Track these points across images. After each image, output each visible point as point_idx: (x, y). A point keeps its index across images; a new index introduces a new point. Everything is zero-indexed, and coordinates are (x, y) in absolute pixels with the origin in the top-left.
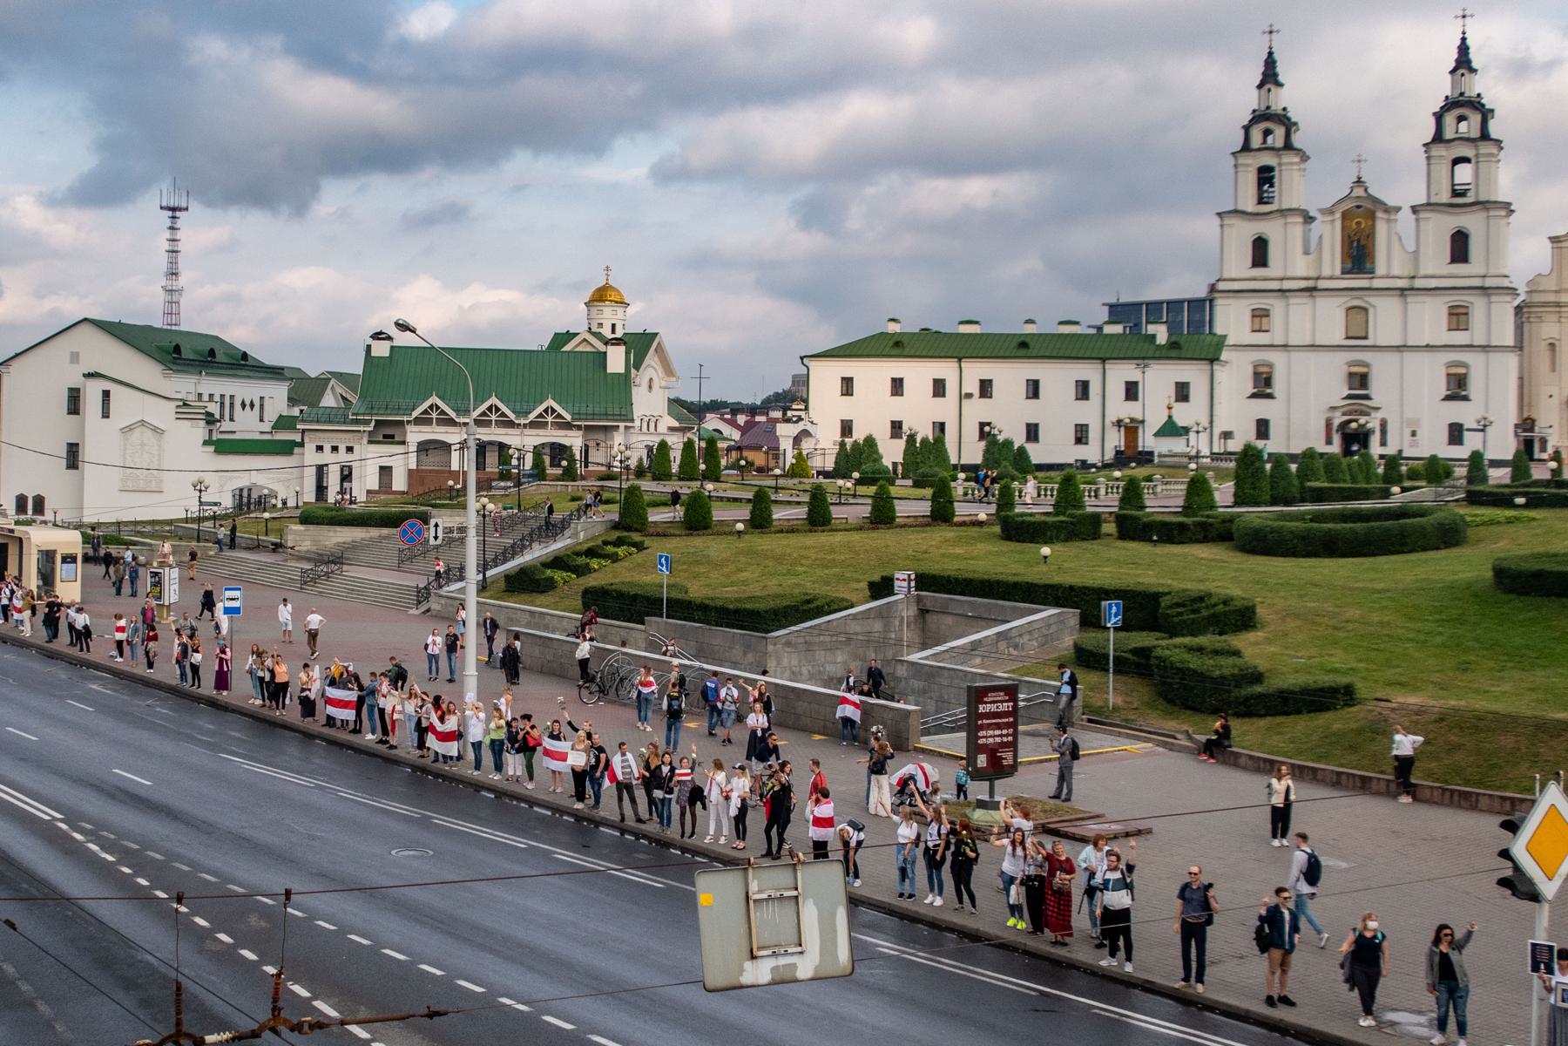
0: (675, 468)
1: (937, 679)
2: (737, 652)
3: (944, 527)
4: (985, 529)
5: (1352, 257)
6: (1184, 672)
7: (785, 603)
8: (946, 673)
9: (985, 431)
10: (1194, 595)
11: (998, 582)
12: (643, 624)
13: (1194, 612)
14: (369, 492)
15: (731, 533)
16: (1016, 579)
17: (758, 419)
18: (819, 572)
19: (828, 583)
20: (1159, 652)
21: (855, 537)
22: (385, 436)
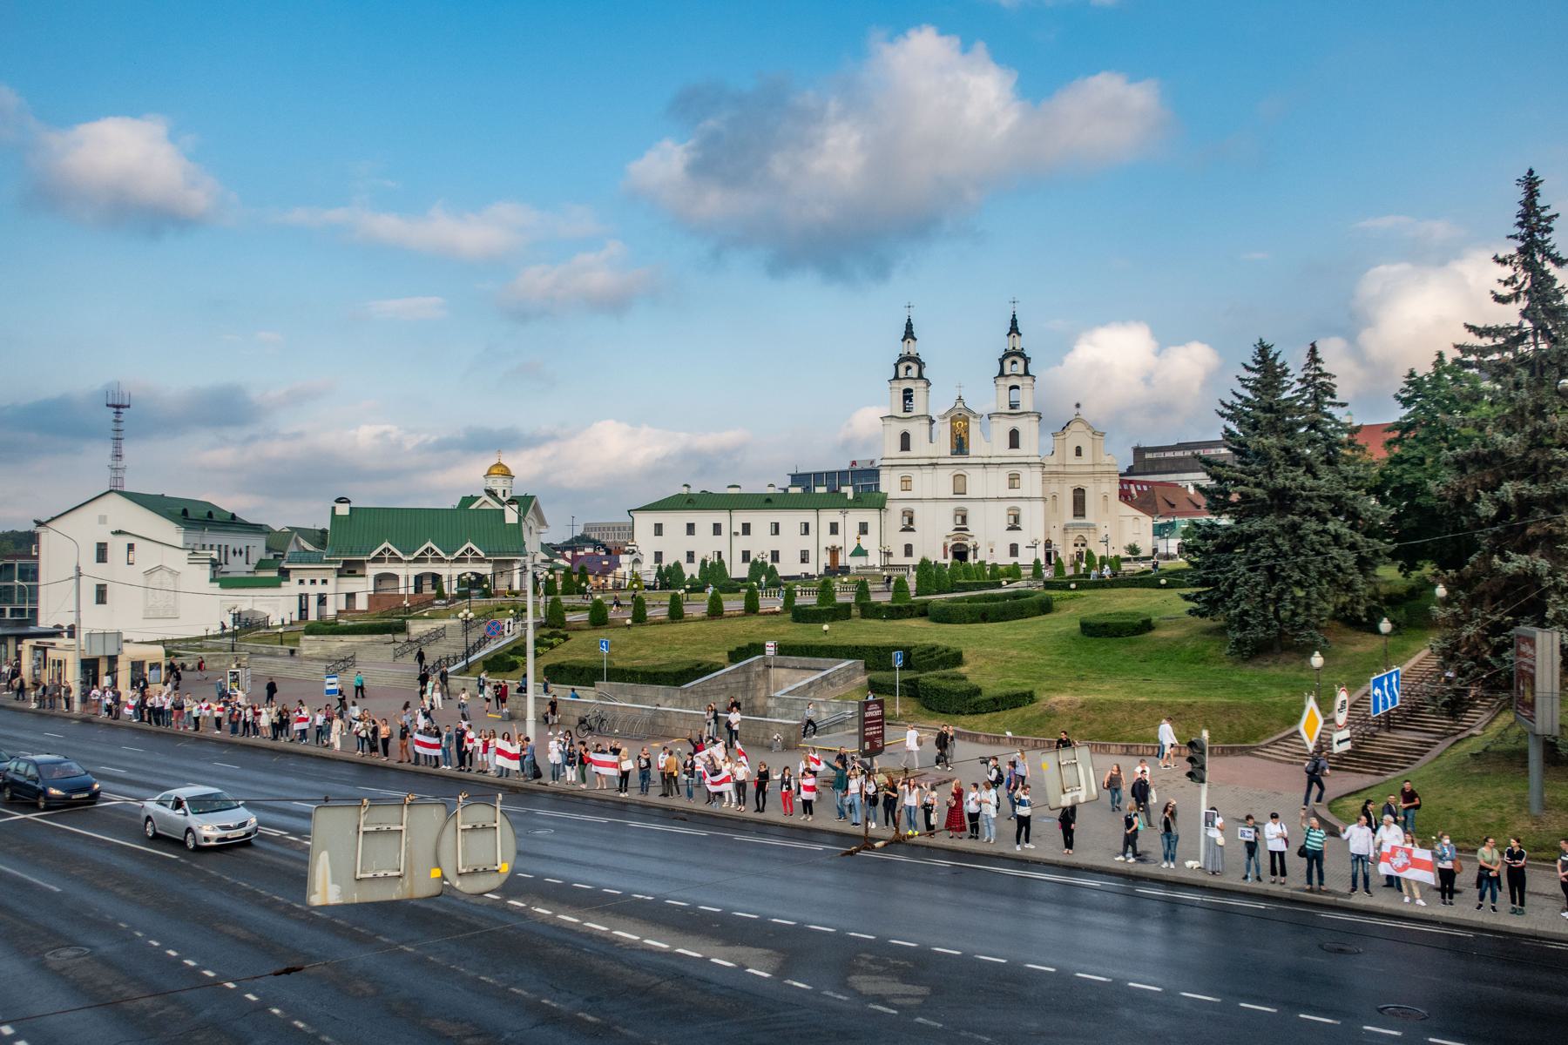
0: (559, 588)
1: (794, 707)
2: (660, 700)
3: (755, 616)
4: (781, 617)
5: (957, 445)
6: (938, 691)
7: (685, 667)
8: (800, 702)
9: (746, 556)
10: (931, 647)
11: (812, 646)
12: (593, 686)
13: (932, 656)
14: (339, 611)
15: (623, 627)
16: (822, 644)
17: (579, 553)
18: (690, 648)
19: (699, 654)
20: (922, 680)
21: (703, 625)
22: (349, 572)
